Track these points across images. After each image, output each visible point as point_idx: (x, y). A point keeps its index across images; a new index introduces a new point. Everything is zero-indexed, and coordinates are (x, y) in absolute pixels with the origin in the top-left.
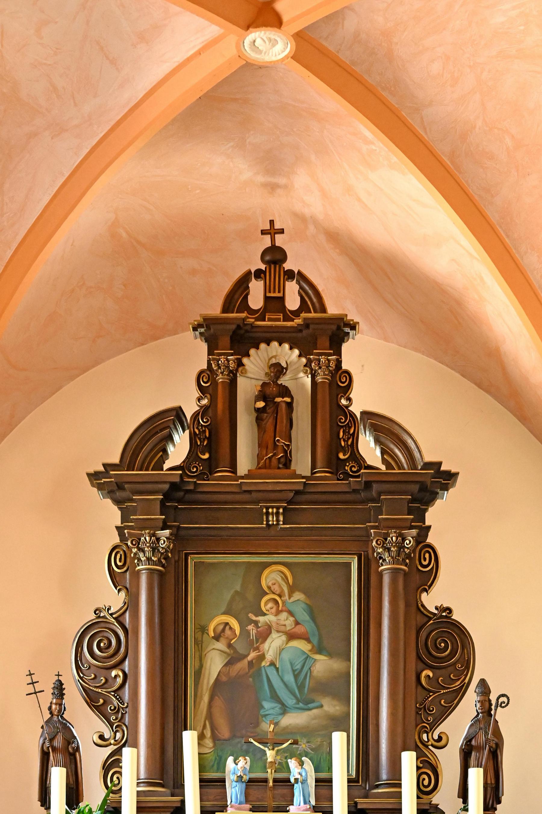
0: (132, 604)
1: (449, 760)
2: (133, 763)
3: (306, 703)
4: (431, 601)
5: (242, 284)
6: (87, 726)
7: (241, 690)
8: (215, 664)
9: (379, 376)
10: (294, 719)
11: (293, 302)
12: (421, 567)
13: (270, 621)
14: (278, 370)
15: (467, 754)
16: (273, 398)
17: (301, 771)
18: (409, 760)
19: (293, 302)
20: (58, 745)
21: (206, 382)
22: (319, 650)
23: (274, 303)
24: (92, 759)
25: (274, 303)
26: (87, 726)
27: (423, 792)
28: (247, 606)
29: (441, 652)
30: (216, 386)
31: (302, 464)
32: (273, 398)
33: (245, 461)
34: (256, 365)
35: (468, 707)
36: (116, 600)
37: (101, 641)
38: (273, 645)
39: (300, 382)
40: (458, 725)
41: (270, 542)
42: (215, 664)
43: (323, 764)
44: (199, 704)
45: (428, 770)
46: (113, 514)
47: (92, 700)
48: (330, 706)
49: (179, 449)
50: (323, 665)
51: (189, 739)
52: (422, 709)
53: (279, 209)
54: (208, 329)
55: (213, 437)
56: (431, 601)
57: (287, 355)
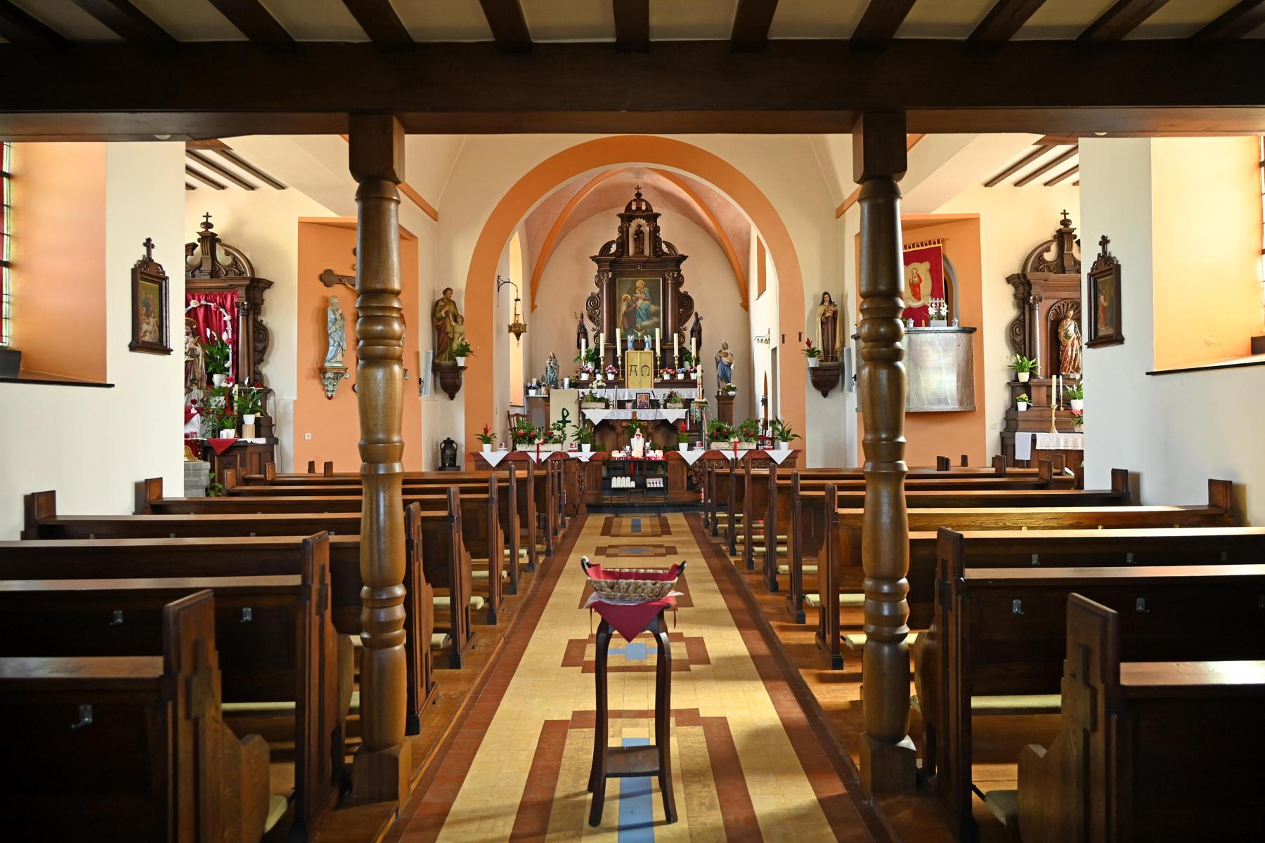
0: (601, 291)
1: (687, 333)
2: (603, 337)
3: (648, 318)
4: (682, 290)
5: (630, 204)
6: (589, 325)
7: (631, 315)
8: (624, 308)
9: (670, 229)
10: (646, 323)
11: (644, 208)
12: (679, 281)
13: (637, 294)
14: (640, 226)
15: (692, 332)
16: (639, 233)
17: (647, 339)
18: (676, 335)
19: (644, 208)
20: (582, 332)
21: (621, 229)
22: (653, 303)
23: (639, 209)
24: (591, 334)
25: (639, 209)
26: (589, 325)
27: (680, 343)
28: (632, 291)
29: (685, 304)
30: (623, 231)
31: (647, 252)
32: (639, 233)
33: (631, 252)
34: (634, 224)
35: (692, 319)
36: (597, 290)
37: (594, 301)
38: (639, 302)
39: (646, 229)
40: (690, 324)
41: (638, 274)
42: (624, 308)
43: (653, 336)
44: (620, 319)
45: (681, 337)
46: (596, 266)
47: (591, 318)
48: (655, 319)
49: (613, 249)
50: (653, 308)
51: (618, 331)
52: (680, 319)
53: (639, 182)
54: (620, 216)
55: (622, 243)
56: (682, 290)
57: (643, 222)
